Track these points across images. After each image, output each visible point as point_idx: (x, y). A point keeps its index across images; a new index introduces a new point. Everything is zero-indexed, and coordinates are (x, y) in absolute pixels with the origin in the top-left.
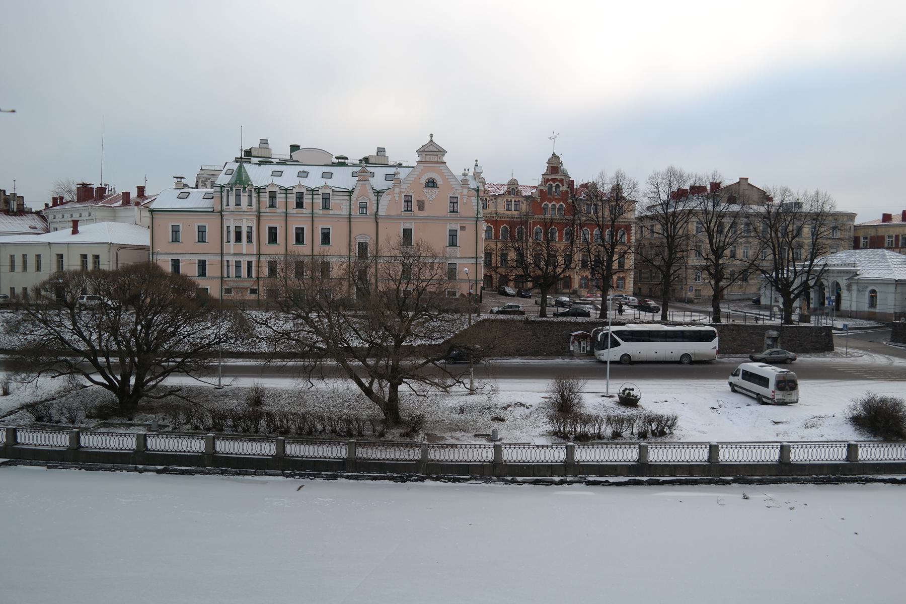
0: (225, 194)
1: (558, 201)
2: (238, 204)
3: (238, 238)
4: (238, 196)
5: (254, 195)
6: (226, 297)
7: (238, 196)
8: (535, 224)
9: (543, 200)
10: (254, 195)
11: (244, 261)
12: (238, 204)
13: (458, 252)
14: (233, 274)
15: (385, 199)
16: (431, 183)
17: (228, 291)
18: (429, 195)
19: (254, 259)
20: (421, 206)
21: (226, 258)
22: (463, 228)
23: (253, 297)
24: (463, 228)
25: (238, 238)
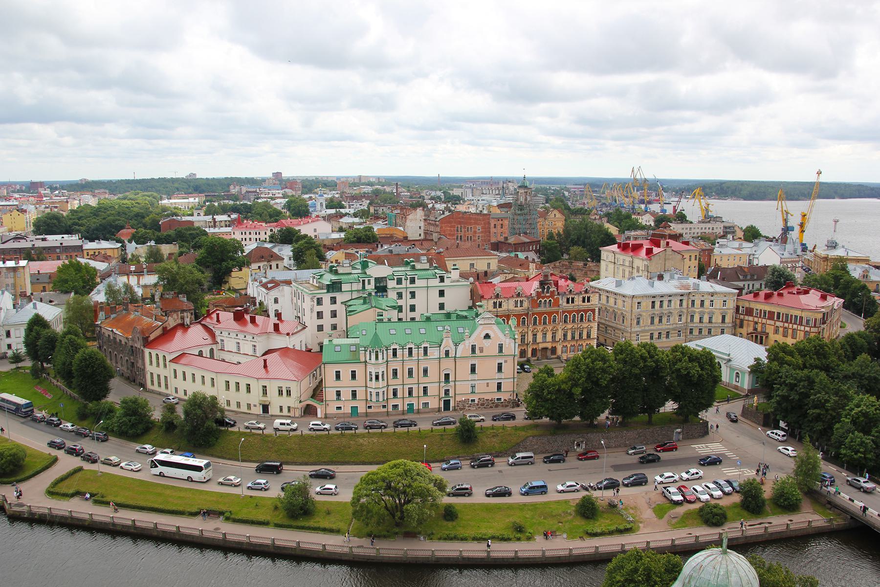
0: (368, 353)
1: (548, 297)
2: (377, 358)
3: (377, 378)
4: (377, 352)
5: (385, 352)
6: (369, 410)
7: (377, 352)
8: (533, 314)
9: (538, 298)
10: (385, 352)
11: (381, 391)
12: (377, 358)
13: (502, 375)
14: (374, 398)
15: (460, 347)
16: (487, 336)
17: (370, 407)
18: (487, 342)
19: (385, 389)
20: (481, 350)
21: (369, 390)
22: (506, 362)
23: (385, 410)
24: (506, 362)
25: (377, 378)
